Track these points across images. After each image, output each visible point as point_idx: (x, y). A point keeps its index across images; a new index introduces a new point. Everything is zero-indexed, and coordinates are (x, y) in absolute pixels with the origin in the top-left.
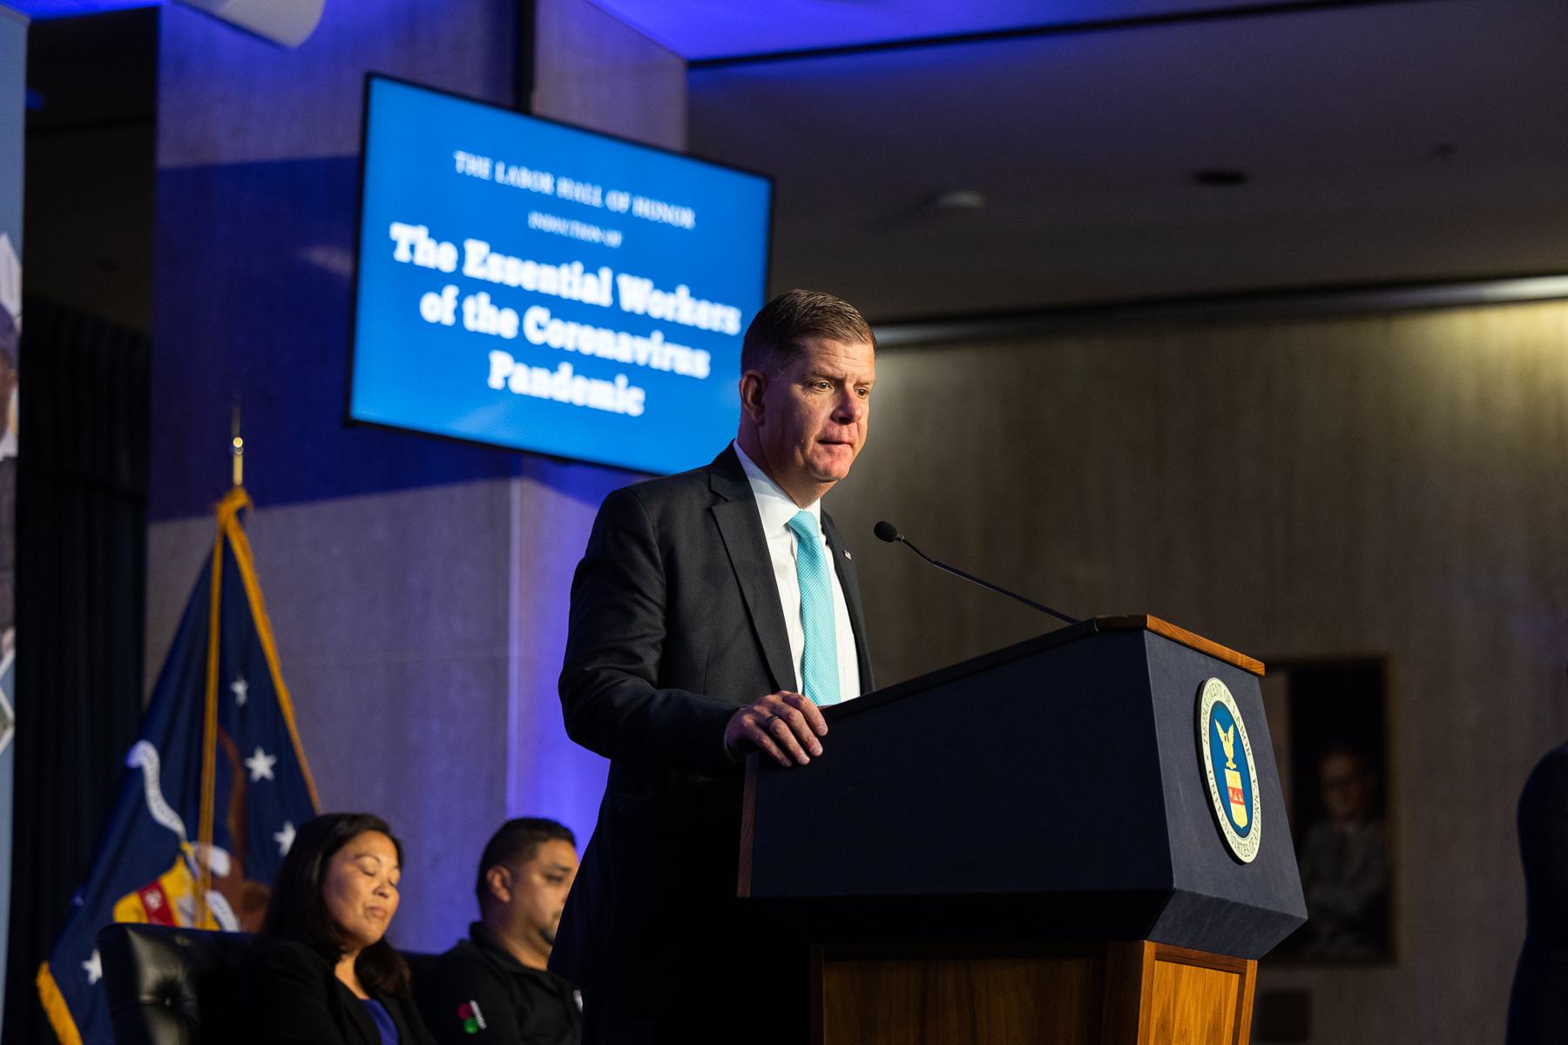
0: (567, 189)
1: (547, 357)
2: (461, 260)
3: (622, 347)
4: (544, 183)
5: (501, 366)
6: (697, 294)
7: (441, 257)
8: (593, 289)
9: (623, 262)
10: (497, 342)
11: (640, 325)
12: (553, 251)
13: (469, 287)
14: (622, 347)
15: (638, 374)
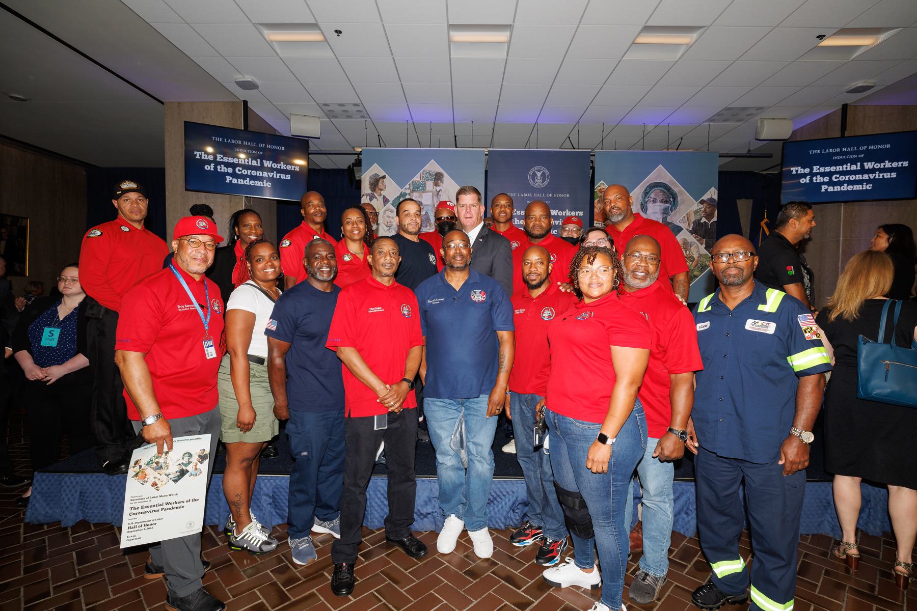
0: (844, 149)
1: (840, 183)
2: (812, 169)
3: (866, 177)
4: (838, 150)
5: (824, 188)
6: (891, 161)
7: (807, 170)
8: (854, 167)
9: (862, 161)
10: (824, 183)
11: (873, 171)
12: (841, 163)
13: (812, 174)
14: (866, 177)
15: (868, 181)
